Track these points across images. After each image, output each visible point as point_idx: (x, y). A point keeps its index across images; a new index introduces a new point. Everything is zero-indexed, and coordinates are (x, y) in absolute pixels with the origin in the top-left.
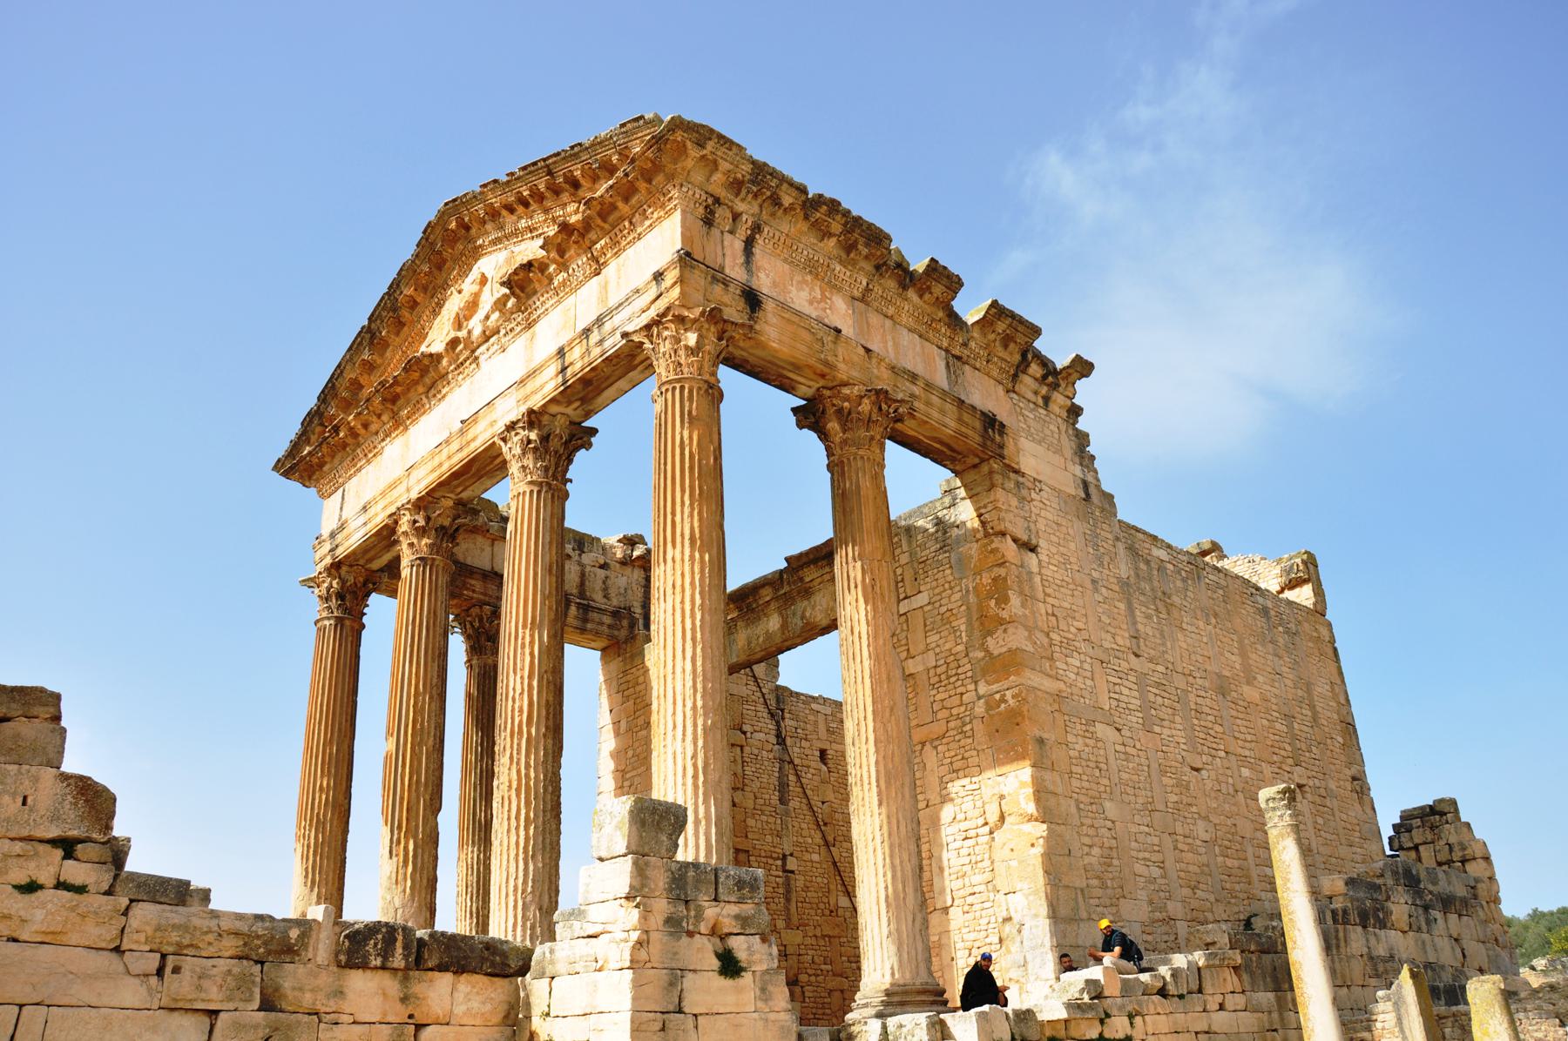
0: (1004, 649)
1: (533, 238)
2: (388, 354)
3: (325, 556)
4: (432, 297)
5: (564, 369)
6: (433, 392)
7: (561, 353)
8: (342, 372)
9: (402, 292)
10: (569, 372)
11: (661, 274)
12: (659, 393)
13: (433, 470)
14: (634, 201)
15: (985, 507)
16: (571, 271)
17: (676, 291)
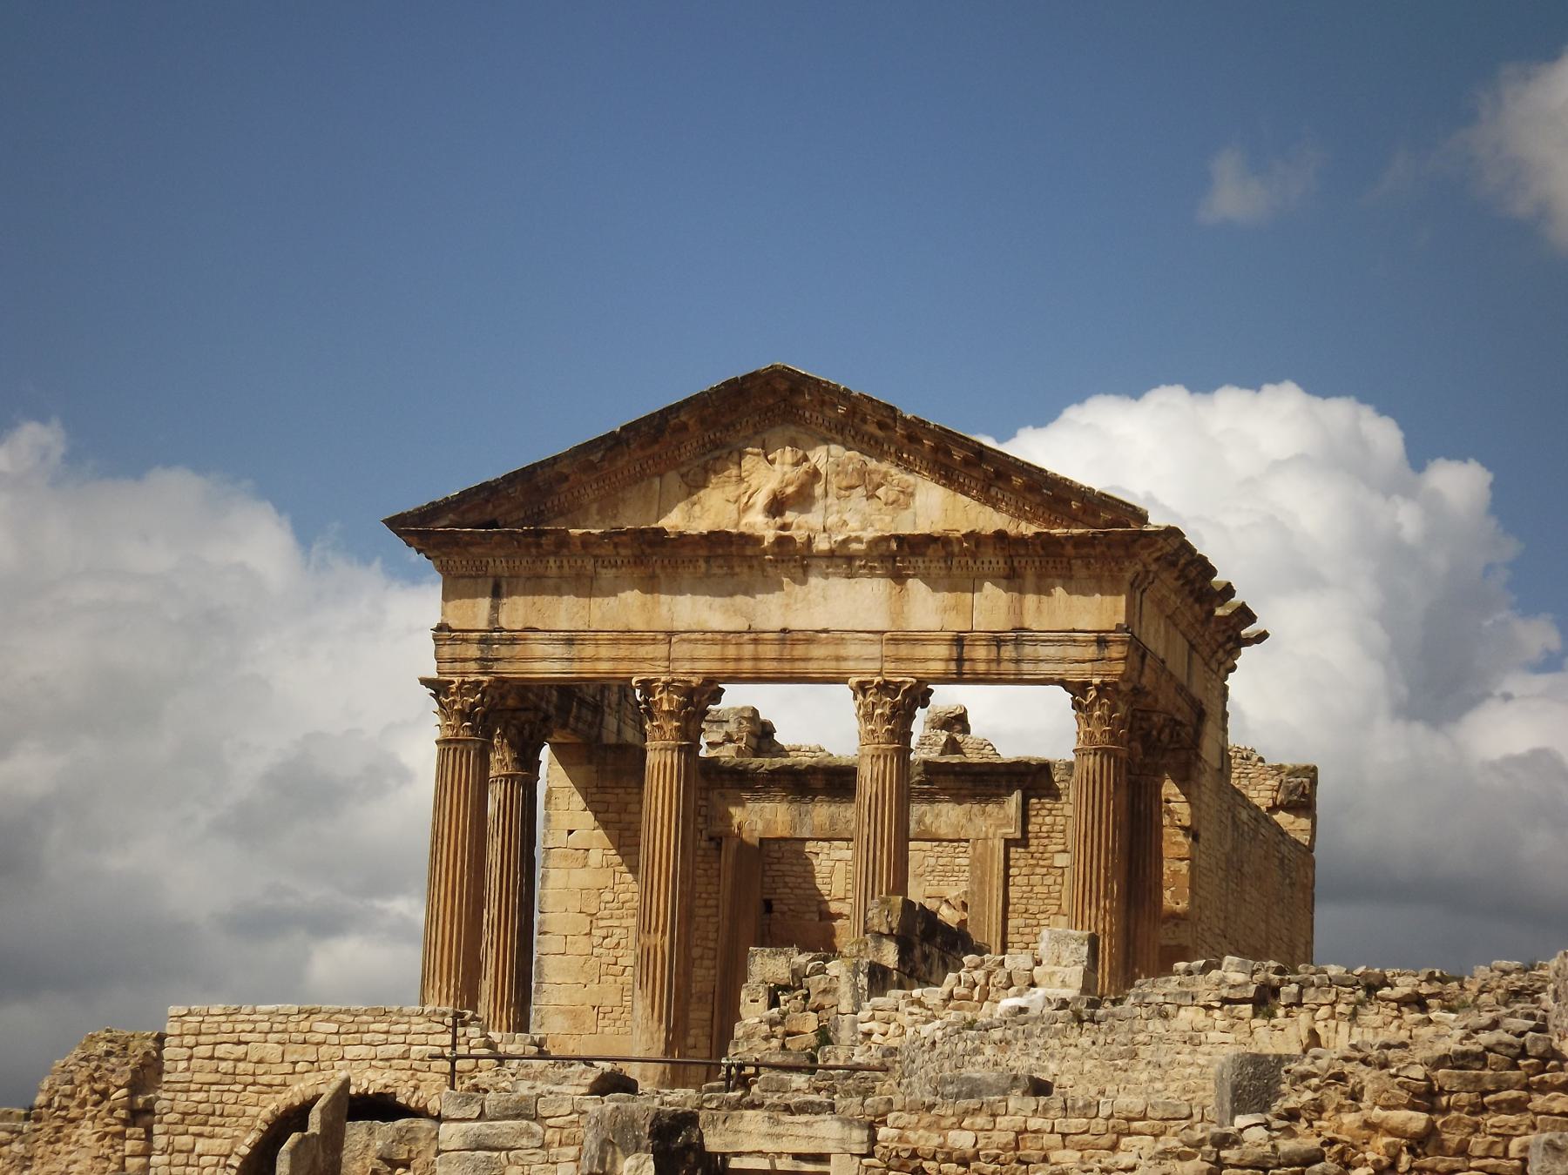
0: (1173, 943)
1: (897, 465)
2: (620, 463)
3: (464, 660)
4: (707, 430)
5: (960, 660)
6: (721, 562)
7: (959, 641)
8: (555, 463)
9: (677, 417)
10: (967, 666)
11: (1109, 642)
12: (1093, 752)
13: (722, 659)
14: (1084, 551)
15: (1176, 795)
16: (978, 563)
17: (1120, 668)
